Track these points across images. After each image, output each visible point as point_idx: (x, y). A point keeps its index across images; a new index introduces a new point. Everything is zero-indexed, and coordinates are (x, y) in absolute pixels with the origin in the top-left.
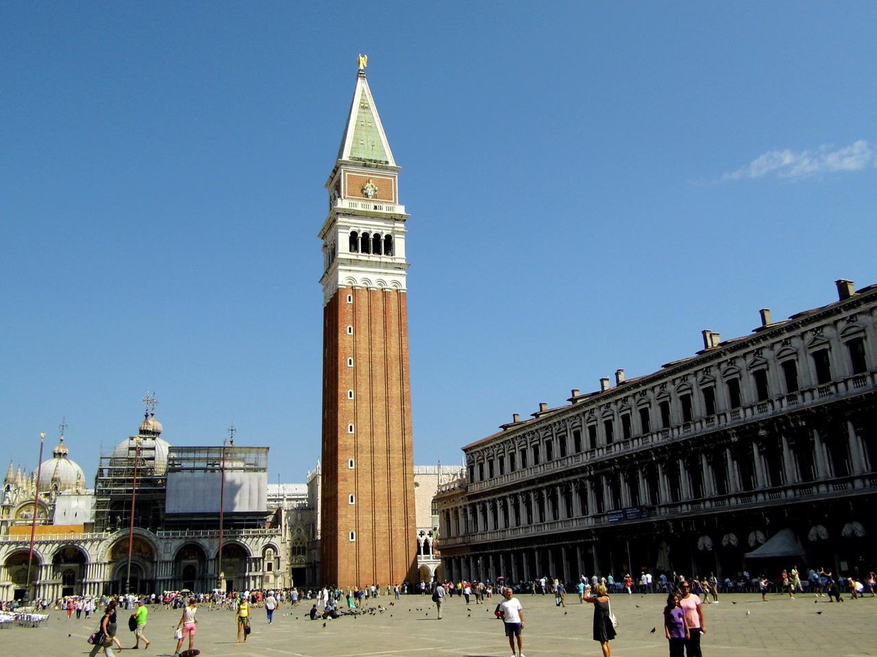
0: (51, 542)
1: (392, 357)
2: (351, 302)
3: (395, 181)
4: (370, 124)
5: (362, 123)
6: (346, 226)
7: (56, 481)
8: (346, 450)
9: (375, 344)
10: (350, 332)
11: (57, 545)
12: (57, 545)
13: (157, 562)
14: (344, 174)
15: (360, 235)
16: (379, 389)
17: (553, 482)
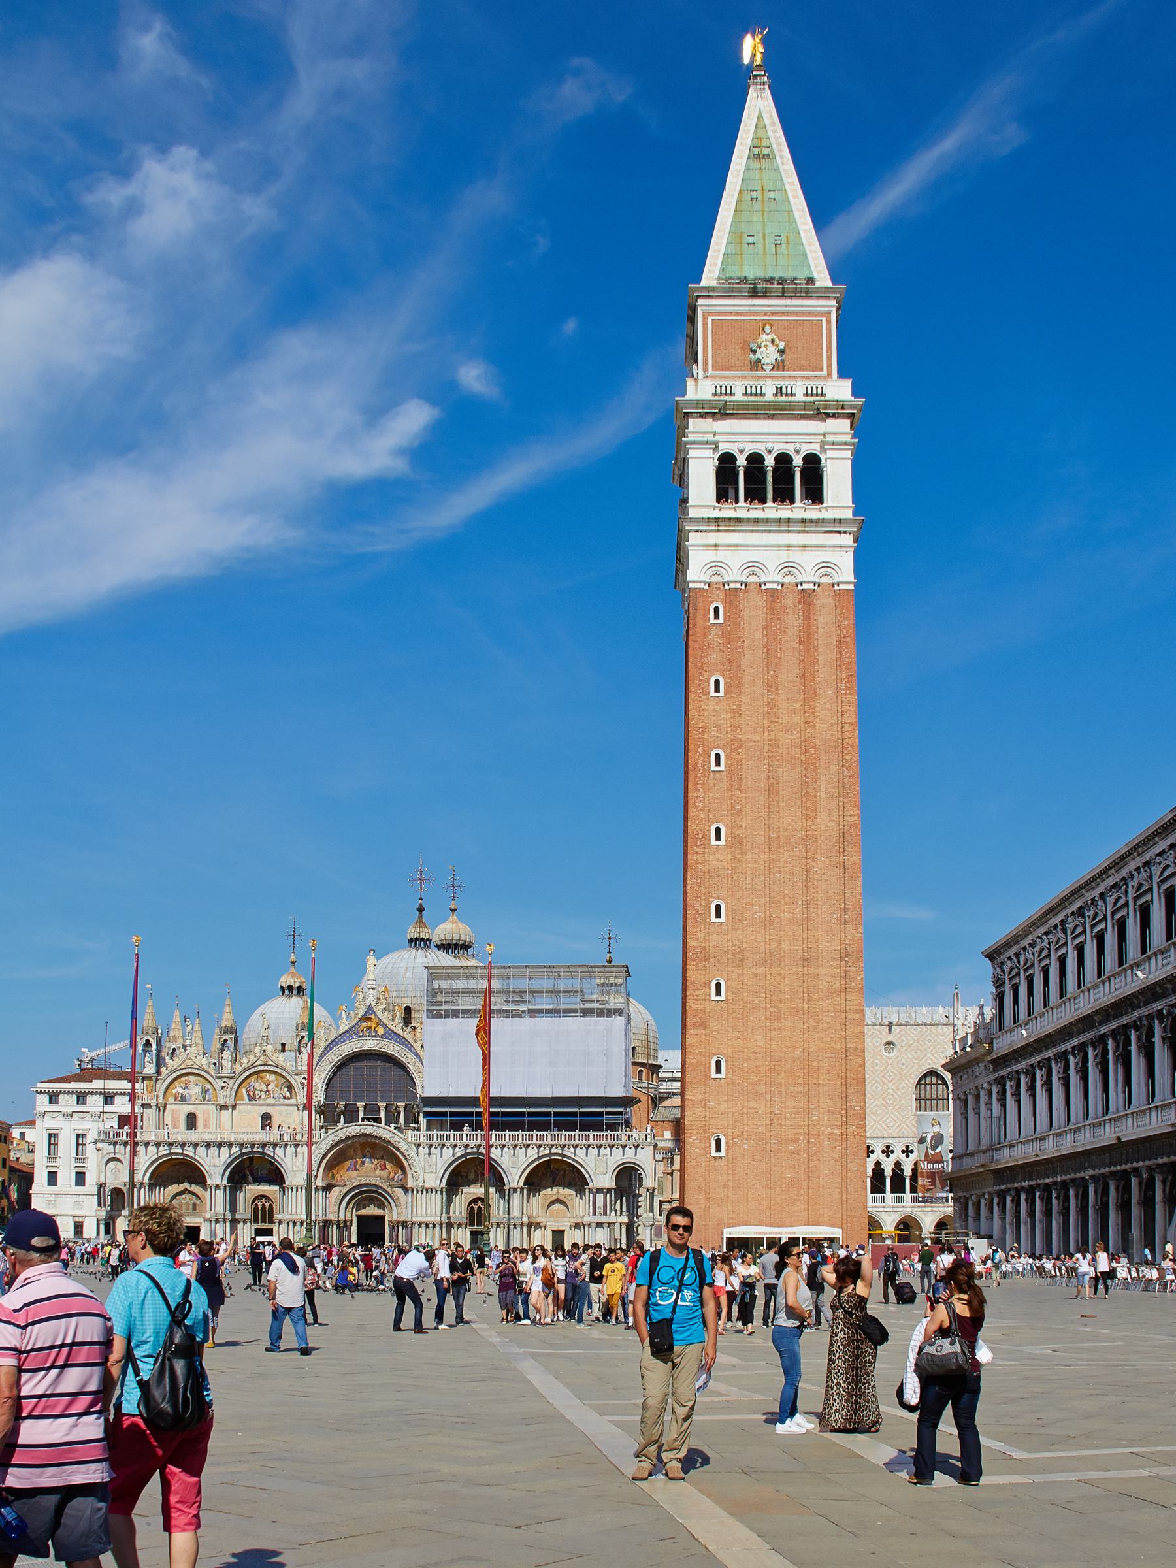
3: (828, 322)
4: (772, 195)
5: (754, 195)
6: (707, 443)
8: (706, 959)
9: (776, 715)
10: (717, 689)
14: (705, 319)
15: (741, 461)
17: (1124, 1020)
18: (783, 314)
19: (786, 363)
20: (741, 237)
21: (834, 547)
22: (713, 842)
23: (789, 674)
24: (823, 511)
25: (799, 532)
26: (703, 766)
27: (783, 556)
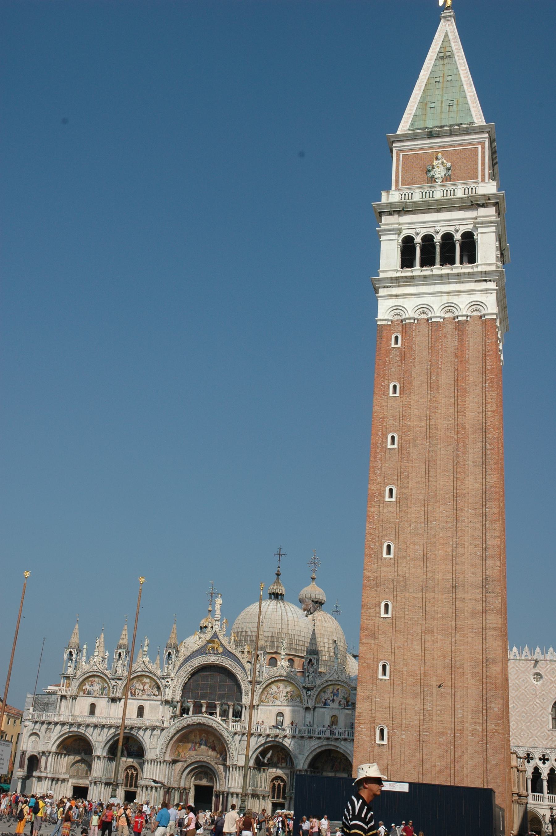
0: (103, 727)
1: (467, 426)
2: (399, 345)
3: (483, 148)
4: (450, 78)
5: (437, 80)
6: (393, 230)
7: (120, 648)
8: (378, 585)
9: (437, 407)
10: (395, 391)
11: (112, 730)
12: (112, 730)
13: (229, 768)
14: (398, 155)
15: (418, 240)
16: (443, 482)
18: (451, 146)
19: (452, 177)
20: (426, 104)
21: (481, 290)
22: (387, 499)
23: (446, 379)
24: (477, 267)
25: (456, 283)
26: (381, 445)
27: (445, 299)
